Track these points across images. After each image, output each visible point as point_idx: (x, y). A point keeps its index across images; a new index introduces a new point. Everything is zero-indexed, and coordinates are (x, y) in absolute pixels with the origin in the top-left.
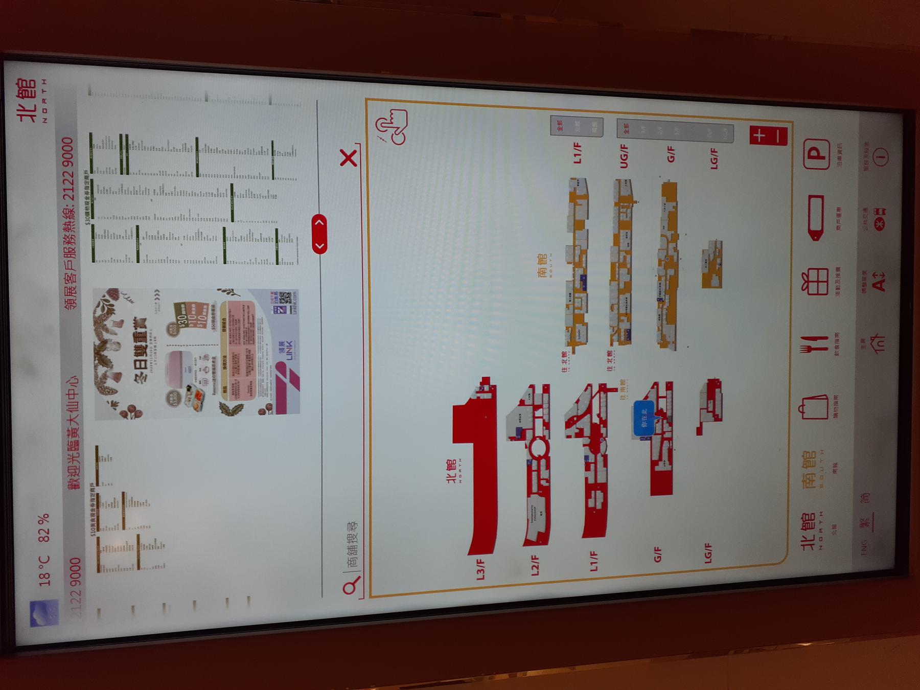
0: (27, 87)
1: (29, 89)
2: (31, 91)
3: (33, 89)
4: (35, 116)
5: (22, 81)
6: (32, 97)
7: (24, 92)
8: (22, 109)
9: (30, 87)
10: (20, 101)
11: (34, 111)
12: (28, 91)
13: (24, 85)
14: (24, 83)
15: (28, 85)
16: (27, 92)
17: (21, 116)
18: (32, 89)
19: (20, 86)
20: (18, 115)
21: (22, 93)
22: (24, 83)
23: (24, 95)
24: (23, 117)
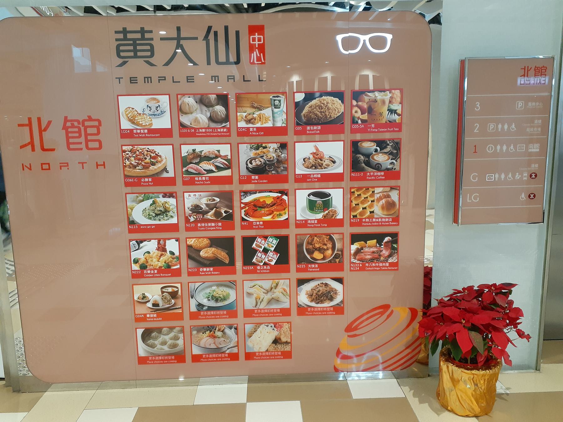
0: (86, 135)
1: (82, 139)
2: (81, 143)
3: (83, 146)
4: (33, 150)
5: (98, 128)
6: (68, 144)
7: (76, 130)
9: (87, 141)
12: (80, 136)
13: (90, 131)
14: (94, 131)
16: (77, 135)
17: (30, 125)
18: (84, 143)
19: (87, 124)
20: (30, 119)
21: (73, 126)
22: (94, 131)
23: (70, 130)
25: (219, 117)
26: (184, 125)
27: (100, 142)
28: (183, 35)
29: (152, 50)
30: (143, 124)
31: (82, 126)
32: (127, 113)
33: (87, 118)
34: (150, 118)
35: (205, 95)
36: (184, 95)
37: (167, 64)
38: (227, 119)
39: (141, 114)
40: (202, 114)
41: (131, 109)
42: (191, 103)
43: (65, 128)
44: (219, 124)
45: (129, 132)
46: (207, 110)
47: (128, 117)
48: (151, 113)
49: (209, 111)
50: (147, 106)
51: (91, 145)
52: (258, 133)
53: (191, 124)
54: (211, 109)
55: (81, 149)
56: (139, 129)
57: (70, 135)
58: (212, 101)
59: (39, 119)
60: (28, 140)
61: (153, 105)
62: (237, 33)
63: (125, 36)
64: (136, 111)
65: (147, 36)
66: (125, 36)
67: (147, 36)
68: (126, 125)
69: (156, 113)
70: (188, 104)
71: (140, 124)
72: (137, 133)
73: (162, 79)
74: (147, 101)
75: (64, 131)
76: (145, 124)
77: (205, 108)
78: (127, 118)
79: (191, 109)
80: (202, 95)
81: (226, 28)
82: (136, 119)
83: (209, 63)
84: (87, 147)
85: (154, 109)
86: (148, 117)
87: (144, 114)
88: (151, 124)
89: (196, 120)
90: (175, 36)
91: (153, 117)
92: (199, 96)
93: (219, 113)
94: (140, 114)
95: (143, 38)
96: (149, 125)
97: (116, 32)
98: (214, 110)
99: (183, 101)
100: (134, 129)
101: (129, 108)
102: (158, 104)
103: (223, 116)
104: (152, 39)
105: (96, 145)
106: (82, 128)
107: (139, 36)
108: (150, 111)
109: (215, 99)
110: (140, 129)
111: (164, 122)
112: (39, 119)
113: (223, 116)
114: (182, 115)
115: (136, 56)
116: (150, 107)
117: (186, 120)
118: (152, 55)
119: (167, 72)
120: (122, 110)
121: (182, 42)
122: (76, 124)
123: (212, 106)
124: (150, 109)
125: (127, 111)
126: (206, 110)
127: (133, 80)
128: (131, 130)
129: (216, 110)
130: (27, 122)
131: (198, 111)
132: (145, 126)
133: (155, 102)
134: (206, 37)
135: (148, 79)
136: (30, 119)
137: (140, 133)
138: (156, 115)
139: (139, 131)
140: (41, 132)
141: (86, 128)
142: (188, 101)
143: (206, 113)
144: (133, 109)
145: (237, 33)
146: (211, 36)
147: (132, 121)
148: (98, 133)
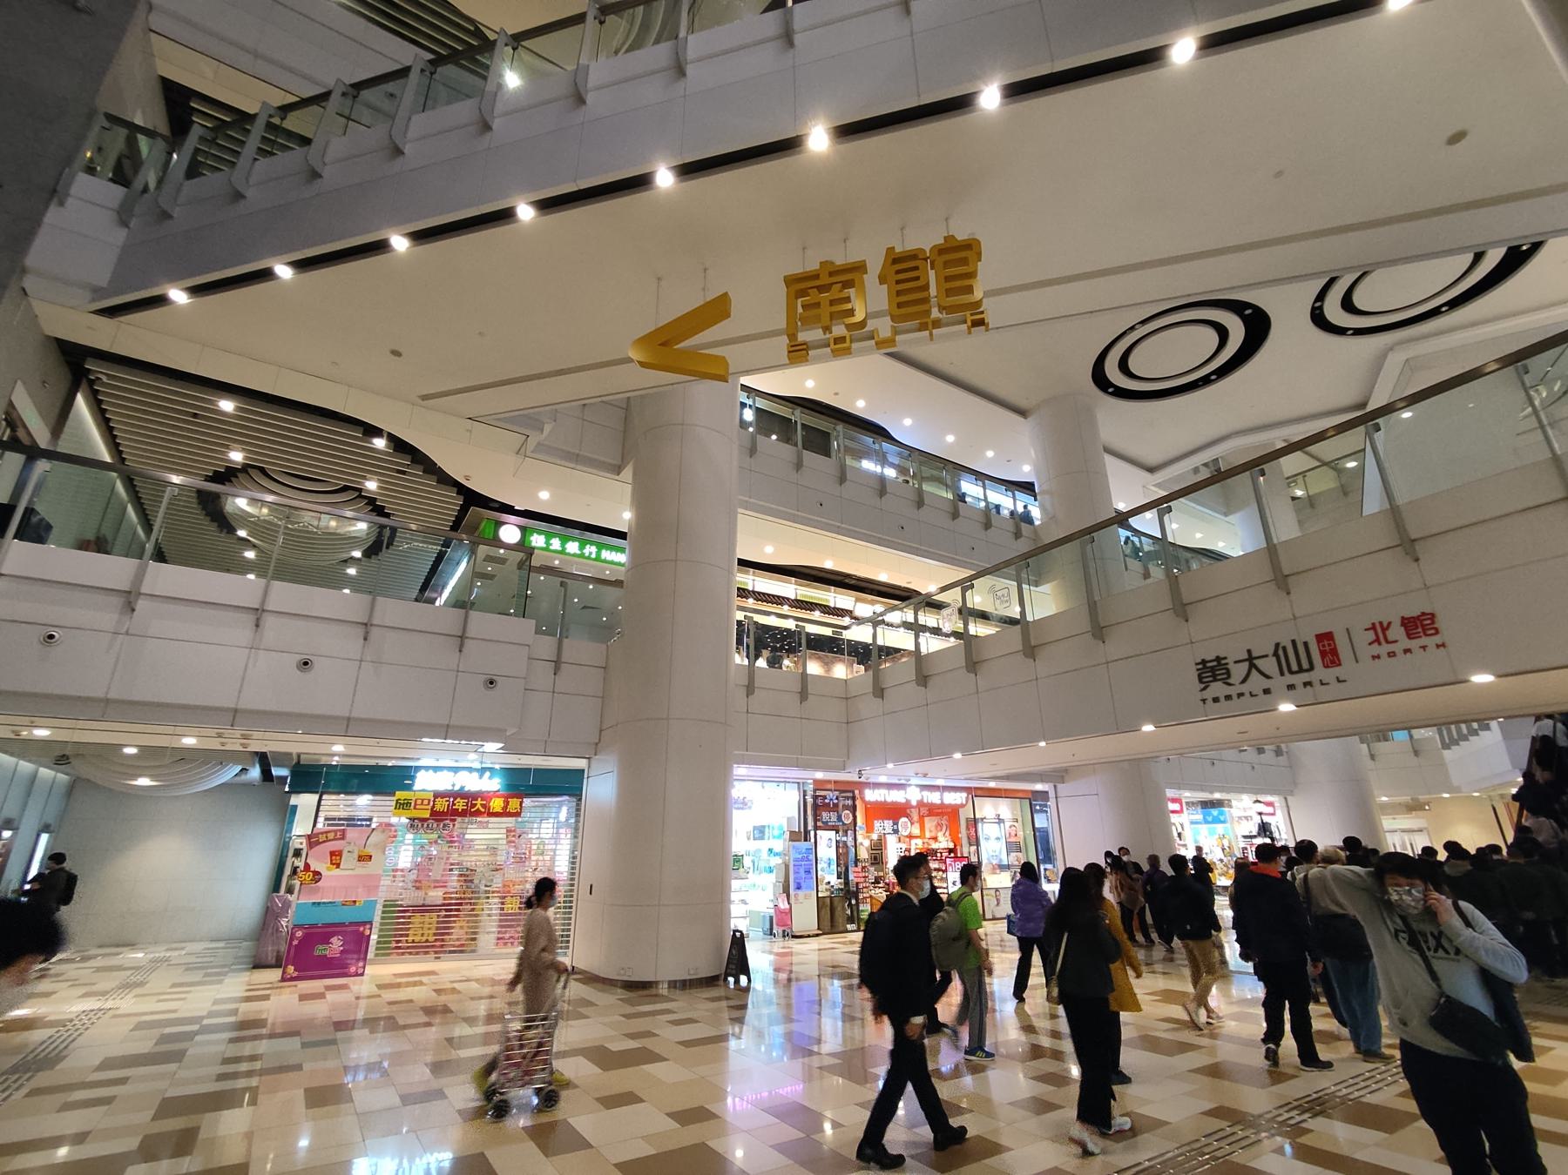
28: (1255, 654)
29: (1228, 673)
37: (1244, 681)
62: (1306, 644)
63: (1204, 666)
65: (1223, 662)
66: (1204, 666)
67: (1223, 662)
73: (1240, 695)
81: (1294, 642)
83: (1282, 674)
90: (1246, 656)
95: (1219, 664)
97: (1197, 664)
104: (1227, 664)
107: (1215, 663)
115: (1215, 680)
118: (1229, 677)
119: (1245, 688)
121: (1256, 662)
127: (1216, 700)
134: (1276, 654)
135: (1228, 697)
145: (1306, 644)
146: (1281, 652)
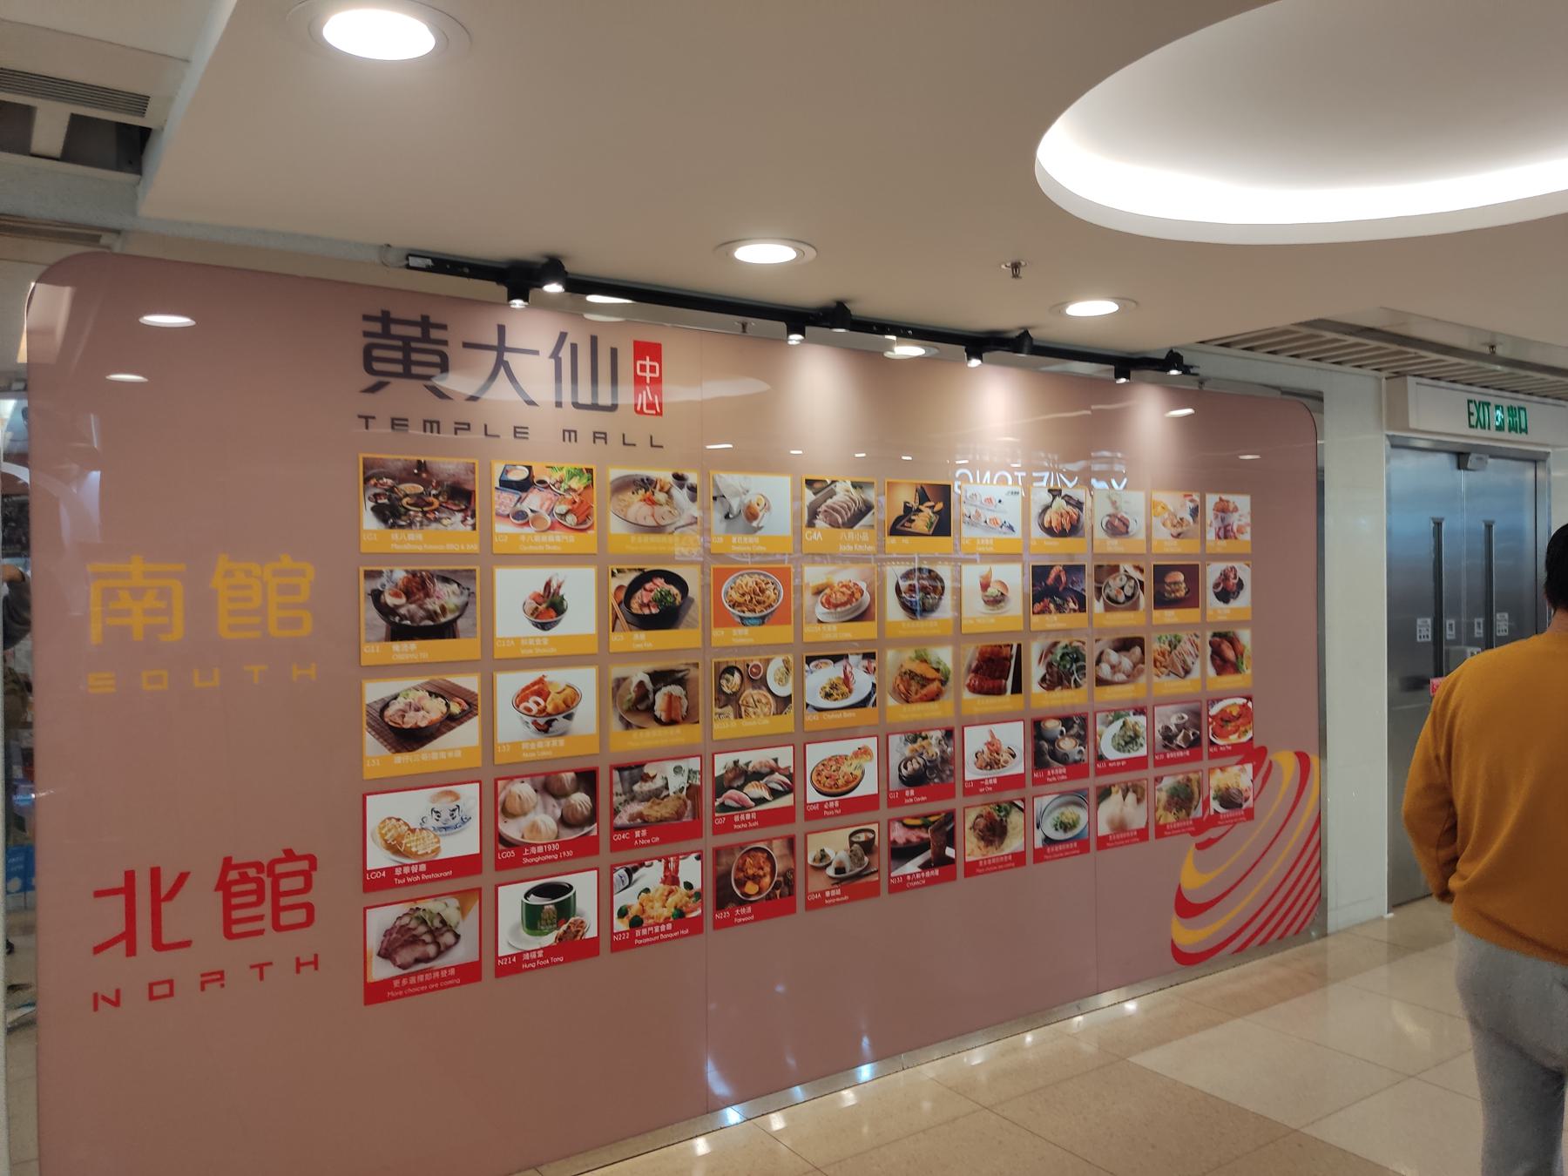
0: (277, 894)
1: (266, 909)
2: (260, 918)
3: (266, 923)
4: (131, 951)
5: (307, 875)
6: (228, 922)
8: (164, 891)
9: (277, 910)
10: (206, 875)
11: (158, 945)
13: (285, 884)
14: (298, 882)
15: (284, 901)
19: (280, 868)
20: (130, 876)
21: (244, 879)
22: (298, 882)
24: (120, 900)
25: (579, 817)
26: (507, 841)
27: (309, 908)
30: (419, 853)
31: (268, 876)
32: (383, 832)
33: (282, 855)
34: (436, 836)
35: (553, 776)
36: (511, 779)
38: (593, 817)
39: (418, 830)
40: (546, 812)
41: (394, 821)
42: (525, 794)
43: (223, 885)
44: (577, 830)
45: (384, 874)
46: (556, 804)
47: (386, 841)
48: (440, 824)
49: (560, 805)
50: (432, 810)
51: (286, 918)
52: (649, 841)
53: (523, 837)
54: (563, 801)
55: (260, 932)
56: (407, 865)
57: (235, 901)
58: (567, 785)
59: (155, 873)
60: (120, 927)
61: (445, 806)
64: (406, 824)
68: (378, 859)
69: (452, 823)
70: (520, 797)
71: (411, 853)
72: (403, 876)
74: (434, 799)
75: (220, 894)
76: (424, 852)
77: (551, 801)
78: (383, 842)
79: (526, 806)
80: (547, 775)
82: (404, 842)
84: (277, 927)
85: (445, 815)
86: (432, 835)
87: (423, 829)
88: (437, 851)
89: (534, 828)
91: (444, 832)
92: (542, 778)
93: (579, 807)
94: (413, 831)
96: (433, 852)
98: (569, 802)
99: (510, 792)
100: (396, 867)
101: (390, 819)
102: (458, 803)
103: (586, 813)
105: (300, 916)
106: (268, 882)
108: (437, 820)
109: (573, 780)
110: (410, 865)
111: (465, 843)
112: (155, 873)
113: (586, 813)
114: (507, 820)
116: (437, 812)
117: (511, 830)
120: (372, 824)
122: (252, 872)
123: (566, 795)
124: (438, 816)
125: (384, 827)
126: (554, 806)
128: (390, 870)
129: (573, 802)
130: (119, 882)
131: (539, 808)
132: (422, 855)
133: (449, 799)
136: (130, 876)
137: (411, 874)
138: (448, 828)
139: (406, 870)
140: (156, 901)
141: (276, 879)
142: (520, 791)
143: (553, 812)
144: (398, 820)
147: (394, 848)
148: (308, 886)
